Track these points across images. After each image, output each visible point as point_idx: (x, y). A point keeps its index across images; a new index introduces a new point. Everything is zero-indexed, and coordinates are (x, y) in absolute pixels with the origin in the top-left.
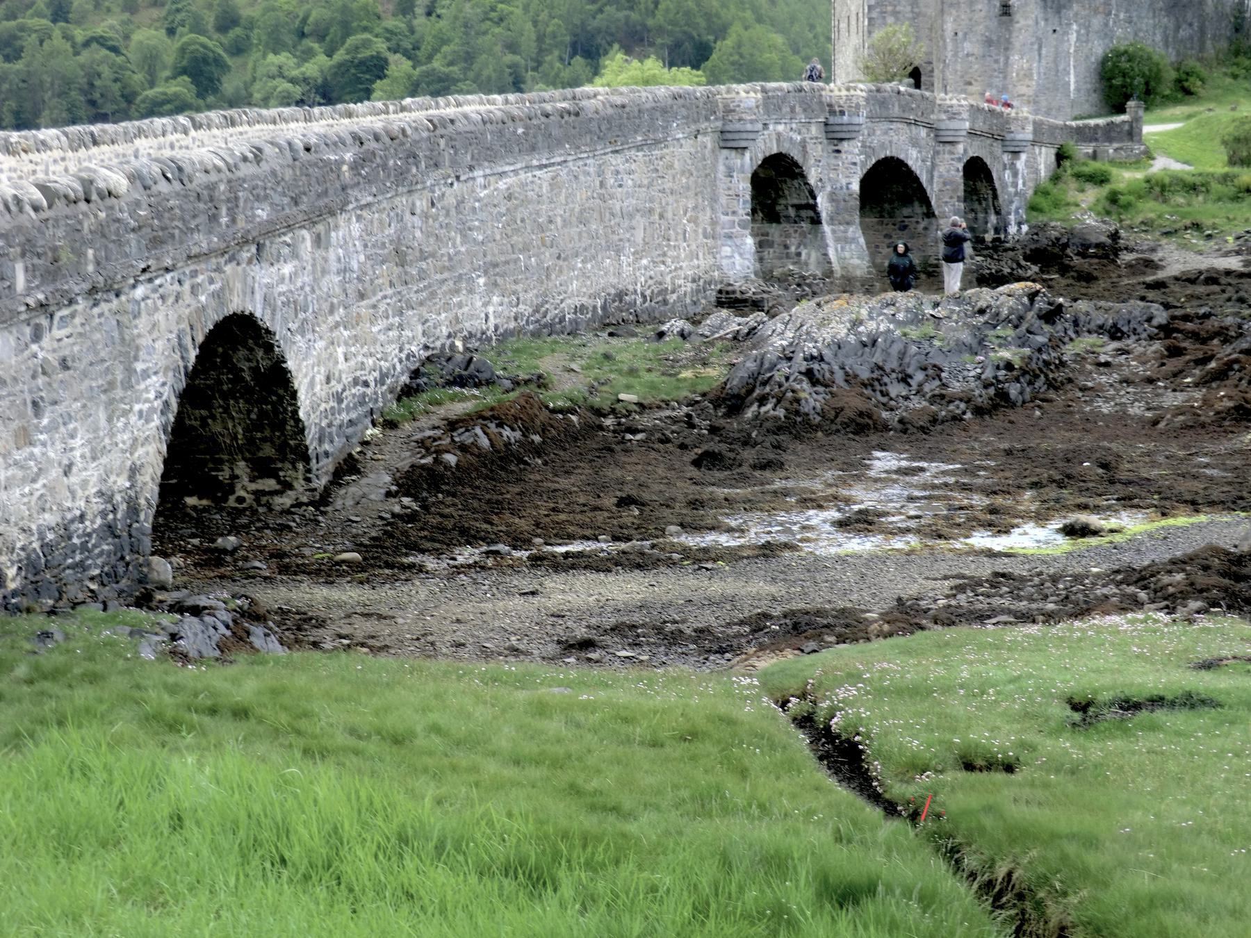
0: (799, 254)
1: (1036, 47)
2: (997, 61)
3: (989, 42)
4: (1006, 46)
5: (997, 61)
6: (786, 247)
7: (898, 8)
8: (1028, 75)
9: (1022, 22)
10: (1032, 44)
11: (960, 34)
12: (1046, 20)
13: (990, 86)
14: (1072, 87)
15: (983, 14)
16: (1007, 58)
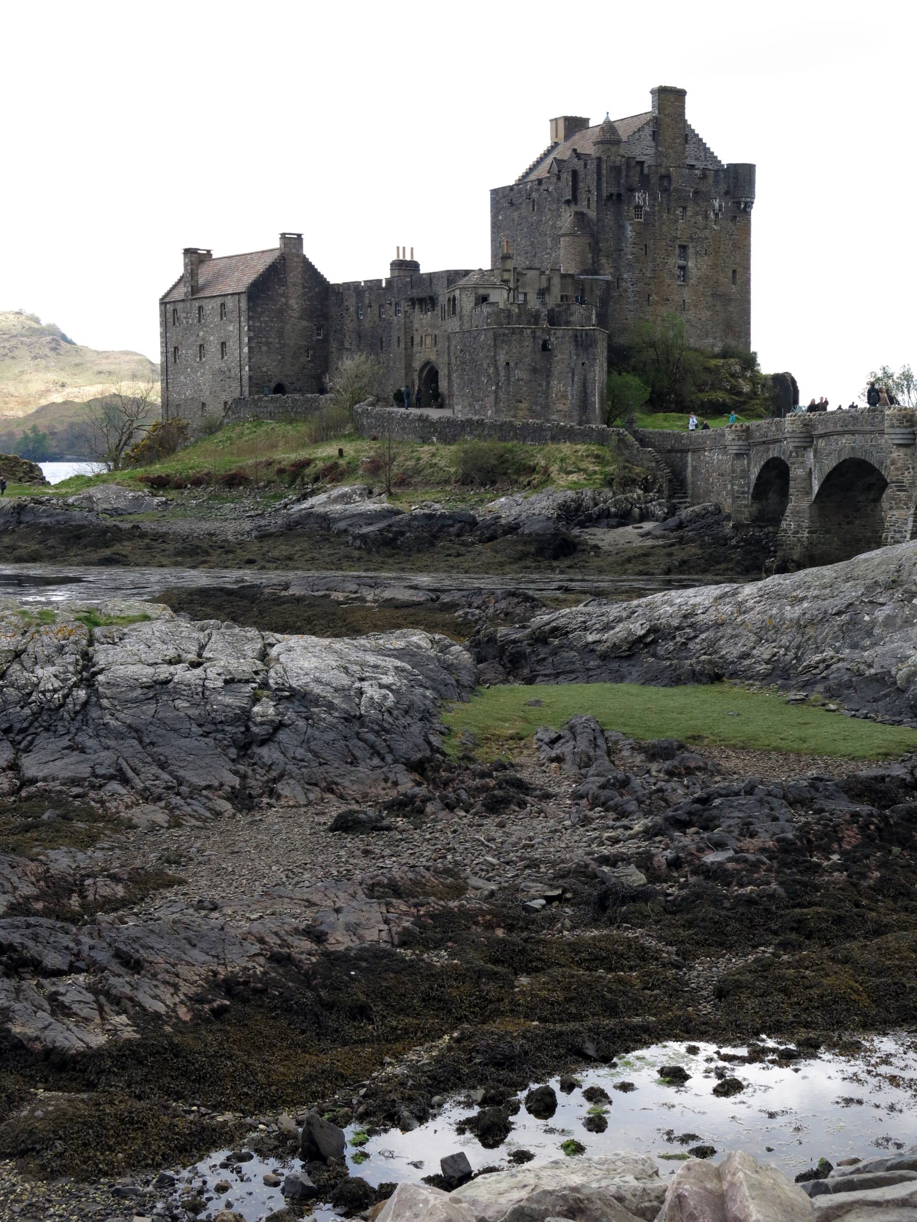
2: (540, 385)
3: (534, 370)
4: (549, 375)
5: (540, 385)
7: (270, 340)
8: (564, 396)
9: (559, 356)
11: (512, 364)
12: (577, 355)
13: (536, 403)
15: (529, 349)
16: (548, 383)
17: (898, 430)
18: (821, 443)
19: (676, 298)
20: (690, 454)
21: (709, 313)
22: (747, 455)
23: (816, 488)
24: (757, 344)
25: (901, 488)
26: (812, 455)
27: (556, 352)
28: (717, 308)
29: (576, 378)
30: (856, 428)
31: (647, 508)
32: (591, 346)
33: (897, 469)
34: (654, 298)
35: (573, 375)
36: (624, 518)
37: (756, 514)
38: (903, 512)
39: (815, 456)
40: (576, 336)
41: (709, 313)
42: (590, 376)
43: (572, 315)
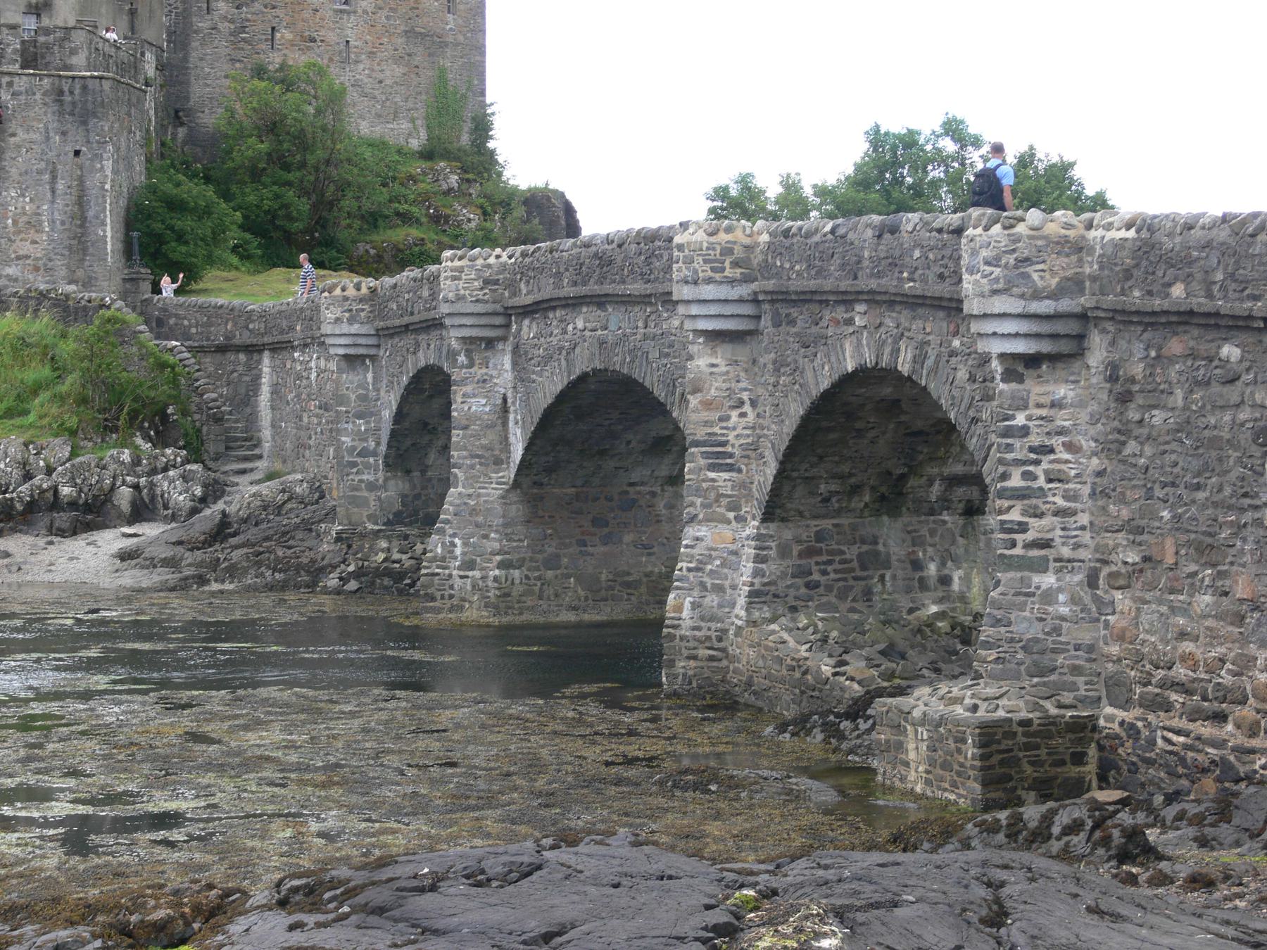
0: (945, 581)
1: (47, 177)
6: (917, 565)
9: (22, 135)
10: (39, 172)
12: (64, 134)
14: (109, 247)
17: (708, 291)
18: (528, 330)
19: (332, 37)
20: (266, 359)
21: (399, 71)
22: (373, 358)
23: (518, 451)
24: (502, 143)
25: (720, 461)
26: (507, 361)
27: (13, 126)
28: (417, 60)
29: (61, 186)
30: (608, 288)
31: (152, 486)
32: (94, 115)
33: (708, 405)
34: (284, 34)
35: (54, 179)
36: (90, 514)
37: (398, 506)
38: (726, 531)
39: (515, 364)
40: (61, 93)
41: (399, 71)
42: (92, 182)
43: (73, 52)
